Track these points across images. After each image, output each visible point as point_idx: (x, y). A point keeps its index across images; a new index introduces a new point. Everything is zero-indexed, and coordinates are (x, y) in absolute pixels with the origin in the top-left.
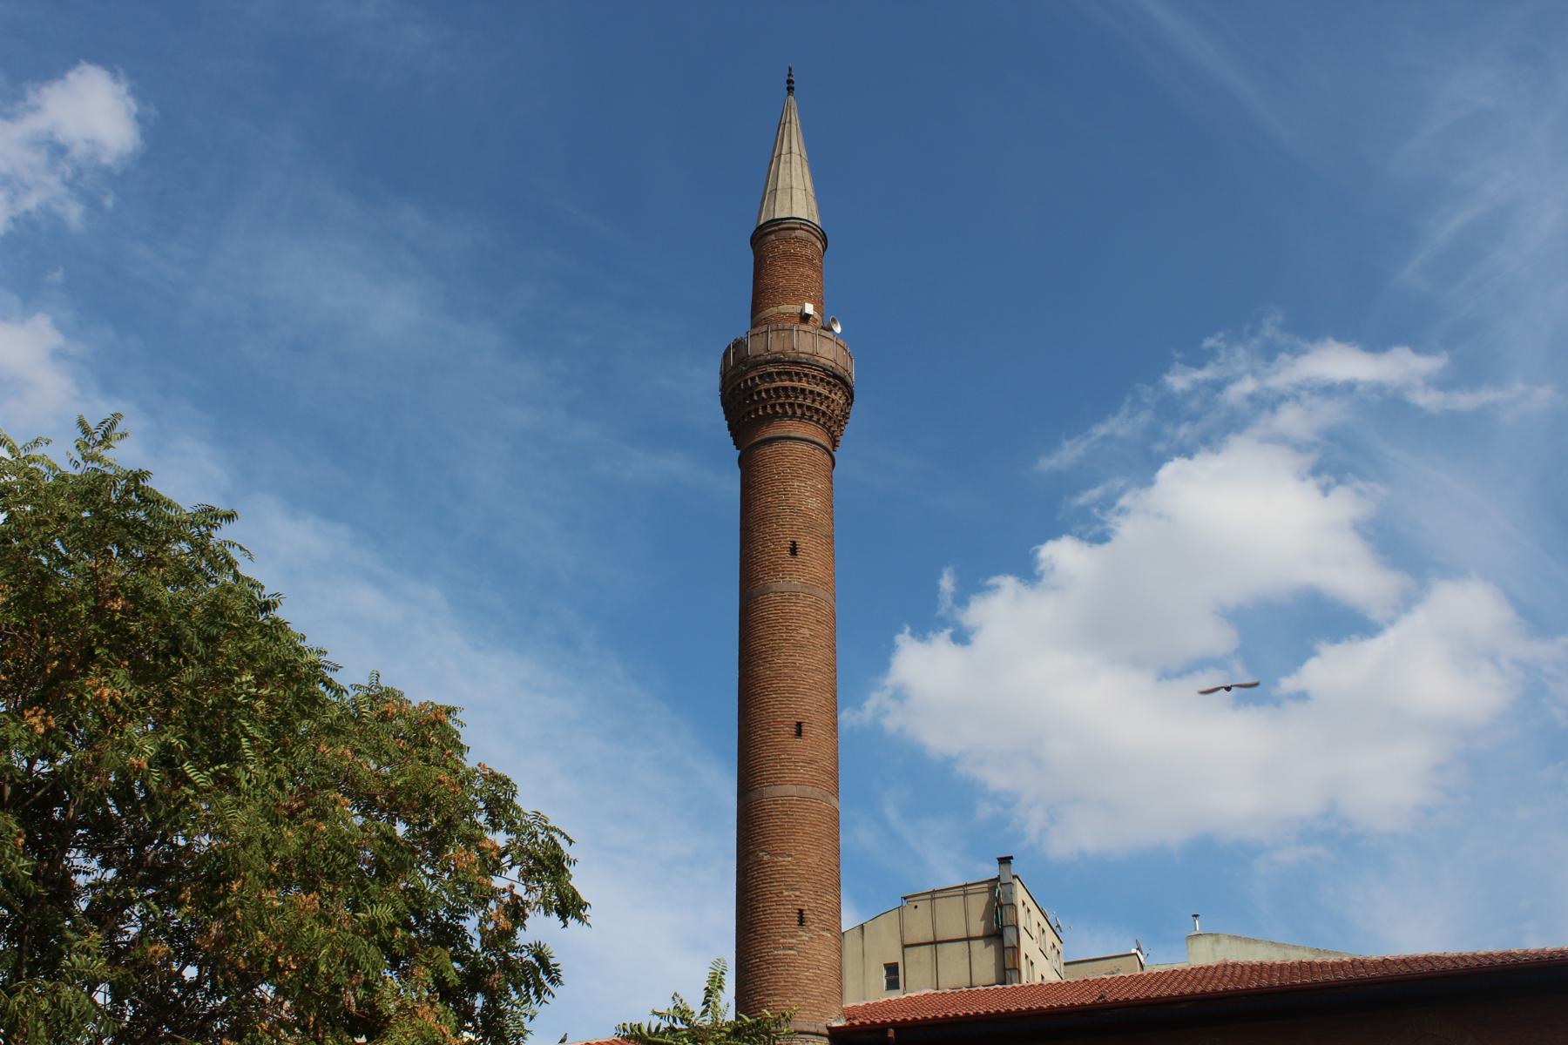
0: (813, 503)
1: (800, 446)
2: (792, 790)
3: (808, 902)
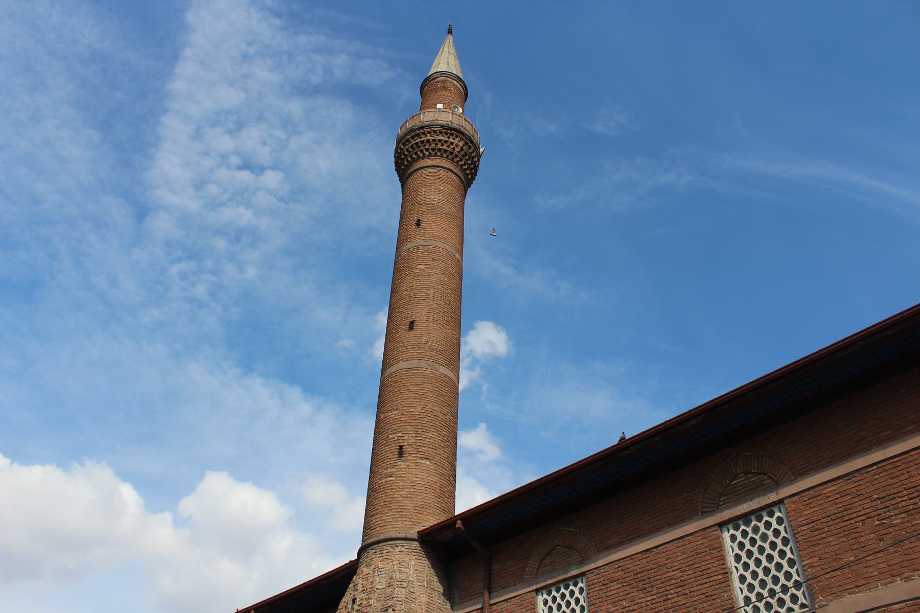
0: (436, 197)
1: (427, 171)
2: (404, 365)
3: (407, 438)
